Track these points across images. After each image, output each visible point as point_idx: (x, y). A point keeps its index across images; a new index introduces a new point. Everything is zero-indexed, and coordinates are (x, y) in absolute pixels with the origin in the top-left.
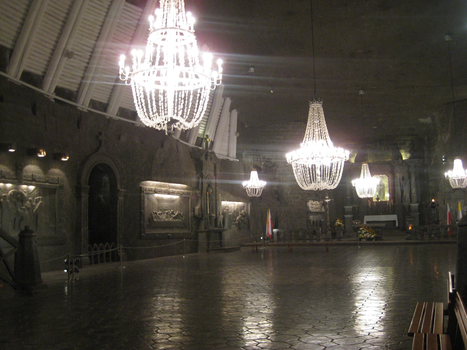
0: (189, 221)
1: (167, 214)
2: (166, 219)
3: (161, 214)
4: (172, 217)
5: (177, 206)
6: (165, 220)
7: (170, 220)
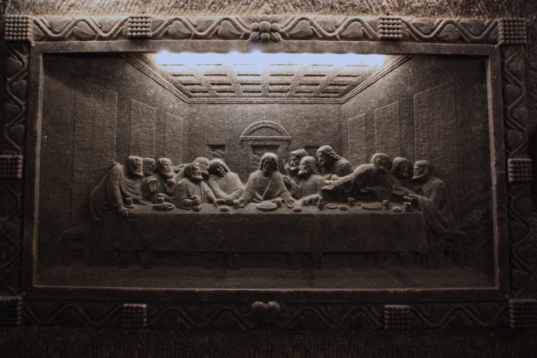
0: (489, 214)
1: (268, 174)
2: (252, 199)
4: (315, 188)
5: (368, 120)
6: (232, 211)
7: (284, 211)
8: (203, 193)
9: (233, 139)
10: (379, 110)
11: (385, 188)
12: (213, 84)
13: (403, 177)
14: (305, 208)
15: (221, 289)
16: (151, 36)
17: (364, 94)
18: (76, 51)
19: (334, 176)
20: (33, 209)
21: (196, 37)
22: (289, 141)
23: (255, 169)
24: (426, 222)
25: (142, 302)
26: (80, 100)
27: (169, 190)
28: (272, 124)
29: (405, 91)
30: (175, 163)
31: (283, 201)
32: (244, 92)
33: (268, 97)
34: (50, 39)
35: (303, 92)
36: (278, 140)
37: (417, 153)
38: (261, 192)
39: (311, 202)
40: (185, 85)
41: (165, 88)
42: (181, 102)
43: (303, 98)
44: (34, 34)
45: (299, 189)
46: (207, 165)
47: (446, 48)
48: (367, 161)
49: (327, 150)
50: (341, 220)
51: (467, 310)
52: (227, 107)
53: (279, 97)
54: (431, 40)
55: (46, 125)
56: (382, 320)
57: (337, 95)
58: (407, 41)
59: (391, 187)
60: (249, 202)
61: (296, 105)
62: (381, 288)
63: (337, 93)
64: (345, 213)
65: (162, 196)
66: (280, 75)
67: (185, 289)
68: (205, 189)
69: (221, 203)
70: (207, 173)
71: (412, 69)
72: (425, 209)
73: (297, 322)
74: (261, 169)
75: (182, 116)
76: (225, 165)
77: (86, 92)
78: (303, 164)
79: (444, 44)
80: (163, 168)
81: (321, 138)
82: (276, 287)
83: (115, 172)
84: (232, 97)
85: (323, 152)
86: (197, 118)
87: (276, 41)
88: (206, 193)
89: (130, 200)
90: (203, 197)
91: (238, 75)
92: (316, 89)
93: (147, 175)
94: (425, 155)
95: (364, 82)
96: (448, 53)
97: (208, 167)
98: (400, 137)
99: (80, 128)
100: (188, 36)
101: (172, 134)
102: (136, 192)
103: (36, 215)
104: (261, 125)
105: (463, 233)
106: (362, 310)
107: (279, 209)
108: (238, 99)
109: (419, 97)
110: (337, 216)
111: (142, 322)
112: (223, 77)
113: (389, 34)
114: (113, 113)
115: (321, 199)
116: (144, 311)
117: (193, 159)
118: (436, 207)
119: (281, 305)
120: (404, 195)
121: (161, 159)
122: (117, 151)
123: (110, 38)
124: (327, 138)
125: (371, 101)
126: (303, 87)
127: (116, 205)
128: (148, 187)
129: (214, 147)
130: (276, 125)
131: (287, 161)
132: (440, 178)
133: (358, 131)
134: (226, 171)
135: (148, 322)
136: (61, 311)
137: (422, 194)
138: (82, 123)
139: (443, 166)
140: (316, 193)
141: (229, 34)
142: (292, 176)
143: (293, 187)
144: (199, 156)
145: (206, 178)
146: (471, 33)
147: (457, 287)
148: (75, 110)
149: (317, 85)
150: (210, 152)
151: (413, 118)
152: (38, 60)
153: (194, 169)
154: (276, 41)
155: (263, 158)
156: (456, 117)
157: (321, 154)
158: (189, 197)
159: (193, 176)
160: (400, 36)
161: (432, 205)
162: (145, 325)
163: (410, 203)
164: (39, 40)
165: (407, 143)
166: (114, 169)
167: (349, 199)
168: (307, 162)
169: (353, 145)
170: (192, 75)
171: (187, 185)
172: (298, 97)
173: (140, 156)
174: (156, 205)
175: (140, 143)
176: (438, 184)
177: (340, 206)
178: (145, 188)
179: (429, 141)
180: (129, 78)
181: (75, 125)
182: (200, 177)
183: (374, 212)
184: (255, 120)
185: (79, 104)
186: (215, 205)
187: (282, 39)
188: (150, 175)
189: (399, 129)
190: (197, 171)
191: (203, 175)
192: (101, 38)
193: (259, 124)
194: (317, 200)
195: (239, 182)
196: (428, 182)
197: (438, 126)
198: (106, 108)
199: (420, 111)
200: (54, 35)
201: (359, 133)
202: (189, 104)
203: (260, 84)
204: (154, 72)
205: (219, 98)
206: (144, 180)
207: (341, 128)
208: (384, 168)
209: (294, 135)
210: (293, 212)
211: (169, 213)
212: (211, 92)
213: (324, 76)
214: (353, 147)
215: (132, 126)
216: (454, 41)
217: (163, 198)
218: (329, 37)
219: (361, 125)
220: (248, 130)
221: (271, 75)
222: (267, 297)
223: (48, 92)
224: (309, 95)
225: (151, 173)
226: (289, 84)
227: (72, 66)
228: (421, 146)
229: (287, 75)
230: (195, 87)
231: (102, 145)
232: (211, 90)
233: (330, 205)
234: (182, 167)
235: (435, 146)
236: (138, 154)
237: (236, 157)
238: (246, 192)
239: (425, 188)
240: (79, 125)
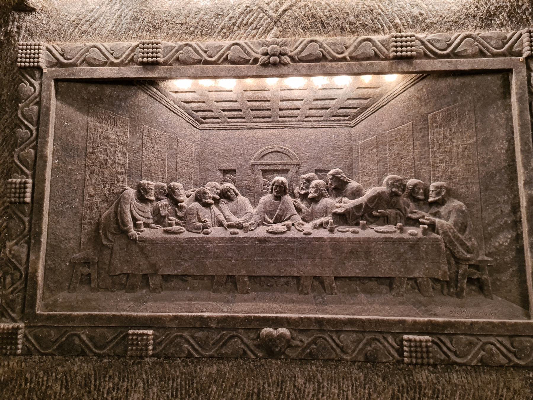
1: (278, 198)
2: (262, 223)
3: (225, 195)
6: (241, 234)
7: (293, 234)
8: (213, 217)
9: (243, 164)
10: (391, 132)
11: (399, 212)
12: (223, 110)
13: (419, 200)
14: (315, 230)
15: (230, 315)
16: (161, 62)
17: (376, 117)
18: (87, 77)
19: (345, 199)
20: (40, 233)
21: (206, 63)
22: (298, 165)
23: (266, 193)
24: (446, 246)
25: (149, 328)
26: (92, 126)
27: (180, 214)
28: (283, 148)
29: (418, 112)
30: (187, 188)
31: (293, 225)
32: (254, 118)
33: (279, 122)
34: (62, 65)
35: (312, 117)
36: (288, 165)
37: (433, 174)
38: (271, 215)
39: (321, 225)
40: (197, 111)
41: (178, 115)
42: (193, 128)
43: (312, 122)
44: (46, 60)
45: (309, 212)
46: (218, 189)
47: (464, 63)
48: (379, 183)
49: (338, 173)
50: (353, 244)
51: (498, 345)
52: (238, 132)
53: (289, 122)
54: (448, 56)
55: (57, 150)
56: (400, 352)
57: (347, 118)
58: (421, 58)
59: (405, 210)
60: (259, 225)
61: (305, 130)
62: (397, 316)
63: (347, 116)
64: (356, 236)
65: (173, 220)
66: (289, 100)
67: (193, 314)
68: (216, 212)
69: (230, 226)
70: (218, 197)
71: (426, 89)
72: (444, 233)
73: (308, 351)
74: (271, 192)
75: (194, 142)
76: (235, 189)
77: (97, 117)
78: (313, 187)
79: (462, 60)
80: (174, 192)
81: (331, 161)
82: (286, 313)
83: (126, 196)
84: (242, 122)
85: (333, 175)
86: (209, 144)
87: (285, 64)
88: (217, 217)
89: (141, 224)
90: (213, 221)
91: (248, 101)
92: (326, 113)
93: (158, 199)
94: (442, 177)
95: (375, 104)
96: (466, 68)
97: (219, 191)
98: (414, 158)
99: (92, 153)
100: (199, 62)
101: (184, 159)
102: (146, 216)
103: (44, 239)
104: (271, 150)
105: (489, 259)
106: (379, 340)
107: (288, 232)
108: (248, 125)
109: (434, 117)
110: (349, 239)
111: (147, 350)
112: (234, 103)
113: (402, 52)
114: (125, 139)
115: (331, 222)
116: (150, 337)
117: (204, 184)
118: (456, 231)
119: (291, 332)
120: (420, 218)
121: (172, 184)
122: (129, 176)
123: (122, 64)
124: (338, 162)
125: (383, 123)
126: (313, 112)
127: (126, 228)
128: (159, 211)
129: (225, 172)
130: (286, 149)
131: (297, 185)
132: (459, 200)
133: (369, 154)
134: (236, 195)
135: (153, 349)
136: (64, 339)
137: (440, 217)
138: (94, 148)
139: (462, 188)
140: (326, 216)
141: (239, 59)
142: (302, 200)
143: (303, 211)
144: (210, 181)
145: (217, 202)
146: (492, 46)
147: (485, 319)
148: (87, 135)
149: (327, 109)
150: (222, 176)
151: (428, 139)
152: (49, 85)
153: (205, 193)
154: (285, 64)
155: (273, 182)
156: (476, 136)
157: (331, 177)
158: (199, 220)
159: (204, 200)
160: (414, 53)
161: (452, 228)
162: (150, 353)
163: (426, 226)
164: (52, 67)
165: (422, 164)
166: (125, 193)
167: (361, 222)
168: (317, 186)
169: (364, 169)
170: (204, 102)
171: (197, 209)
172: (308, 121)
173: (152, 181)
174: (166, 228)
175: (152, 168)
176: (458, 206)
177: (351, 229)
178: (156, 212)
179: (446, 162)
180: (142, 104)
181: (86, 150)
182: (211, 201)
183: (387, 235)
184: (265, 145)
185: (91, 129)
186: (225, 228)
187: (290, 63)
188: (162, 199)
189: (412, 150)
190: (207, 195)
191: (214, 199)
192: (112, 64)
193: (269, 149)
194: (327, 223)
195: (250, 206)
196: (446, 205)
197: (456, 146)
198: (118, 134)
199: (435, 131)
200: (66, 61)
201: (370, 156)
202: (201, 130)
203: (270, 110)
204: (166, 99)
205: (230, 124)
206: (155, 204)
207: (351, 151)
208: (397, 190)
209: (303, 159)
210: (304, 236)
211: (179, 236)
212: (222, 118)
213: (333, 99)
214: (364, 170)
215: (144, 152)
216: (474, 56)
217: (174, 222)
218: (339, 58)
219: (372, 148)
220: (259, 155)
221: (281, 101)
222: (276, 323)
223: (60, 118)
224: (319, 119)
225: (162, 197)
226: (298, 109)
227: (85, 92)
228: (438, 167)
229: (297, 100)
230: (206, 113)
231: (114, 170)
232: (221, 116)
233: (341, 228)
234: (193, 191)
235: (452, 167)
236: (150, 179)
237: (247, 182)
238: (256, 216)
239: (443, 210)
240: (91, 150)
